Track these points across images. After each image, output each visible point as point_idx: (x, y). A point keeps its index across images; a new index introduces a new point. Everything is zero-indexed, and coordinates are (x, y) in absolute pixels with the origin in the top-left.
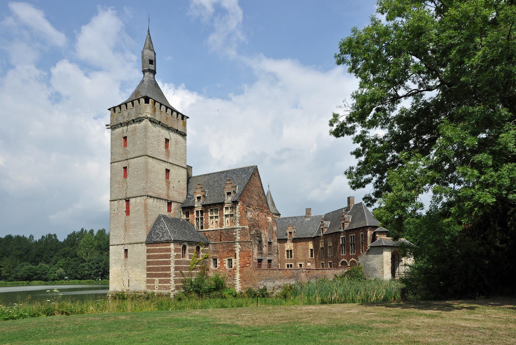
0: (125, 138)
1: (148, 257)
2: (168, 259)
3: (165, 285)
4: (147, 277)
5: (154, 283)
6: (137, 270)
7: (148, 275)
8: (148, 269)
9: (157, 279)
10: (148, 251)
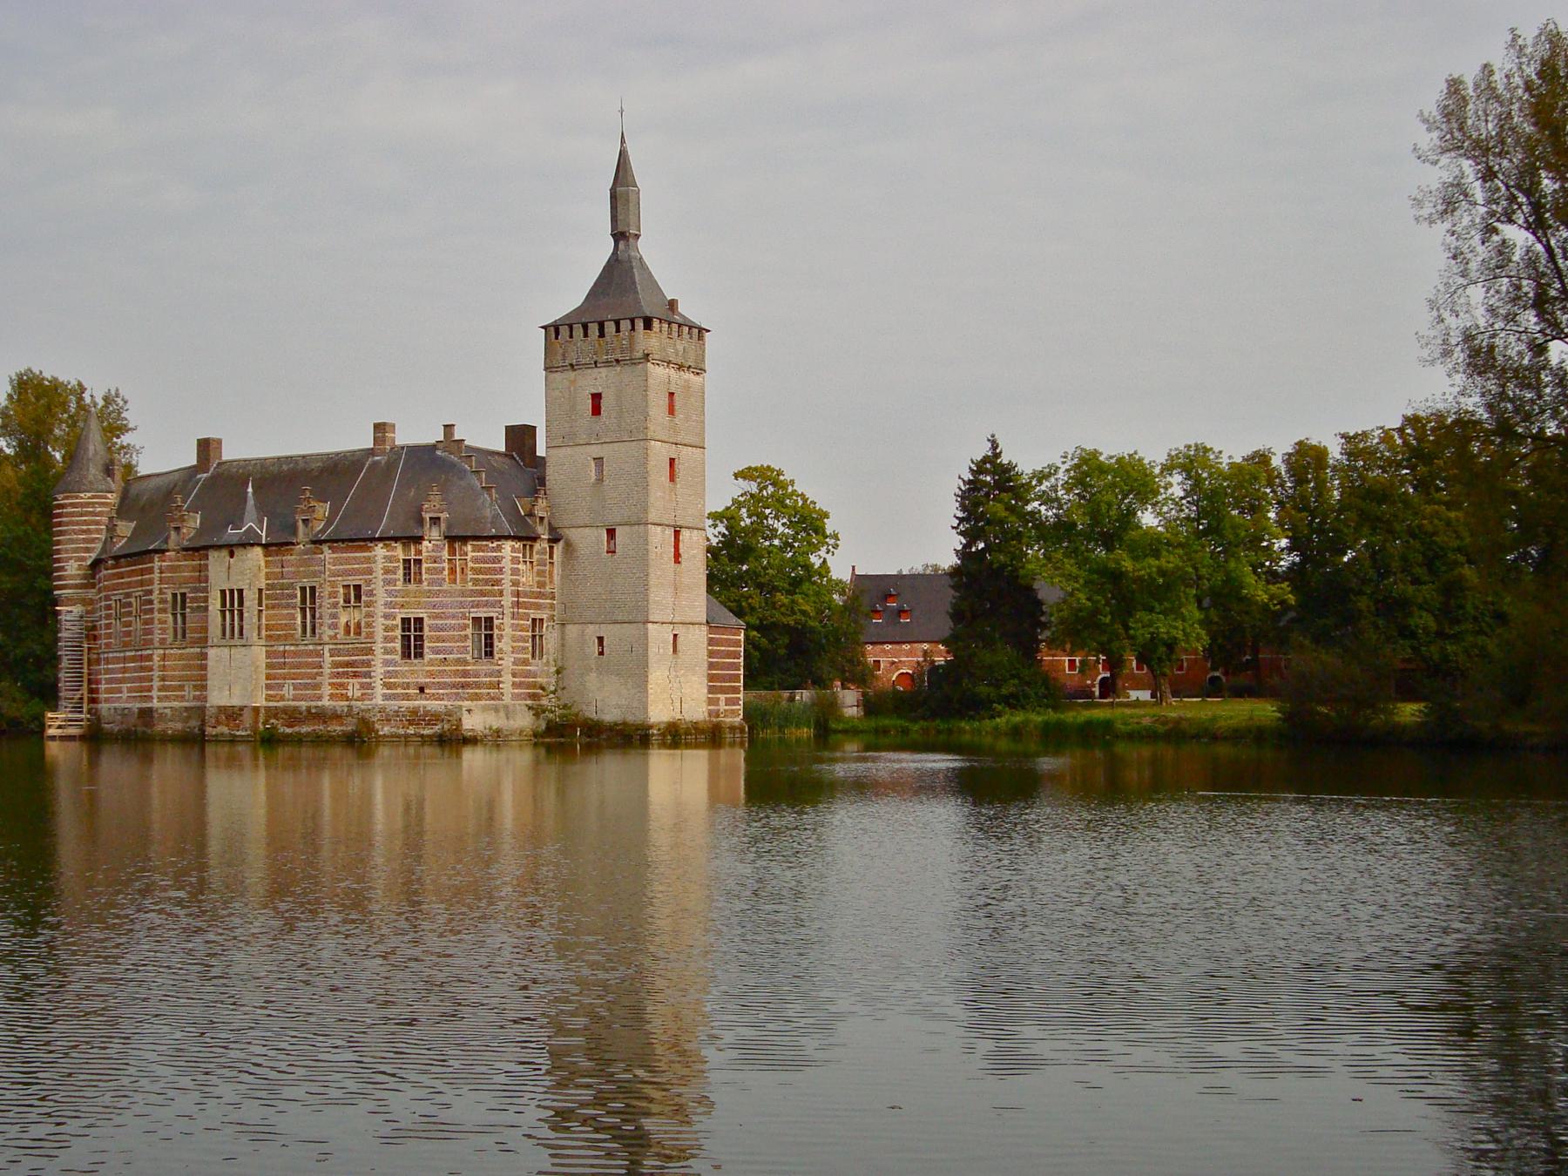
0: (672, 394)
1: (711, 654)
2: (736, 661)
3: (734, 707)
4: (709, 692)
5: (718, 705)
6: (694, 678)
7: (711, 690)
8: (711, 678)
9: (722, 697)
10: (711, 642)
